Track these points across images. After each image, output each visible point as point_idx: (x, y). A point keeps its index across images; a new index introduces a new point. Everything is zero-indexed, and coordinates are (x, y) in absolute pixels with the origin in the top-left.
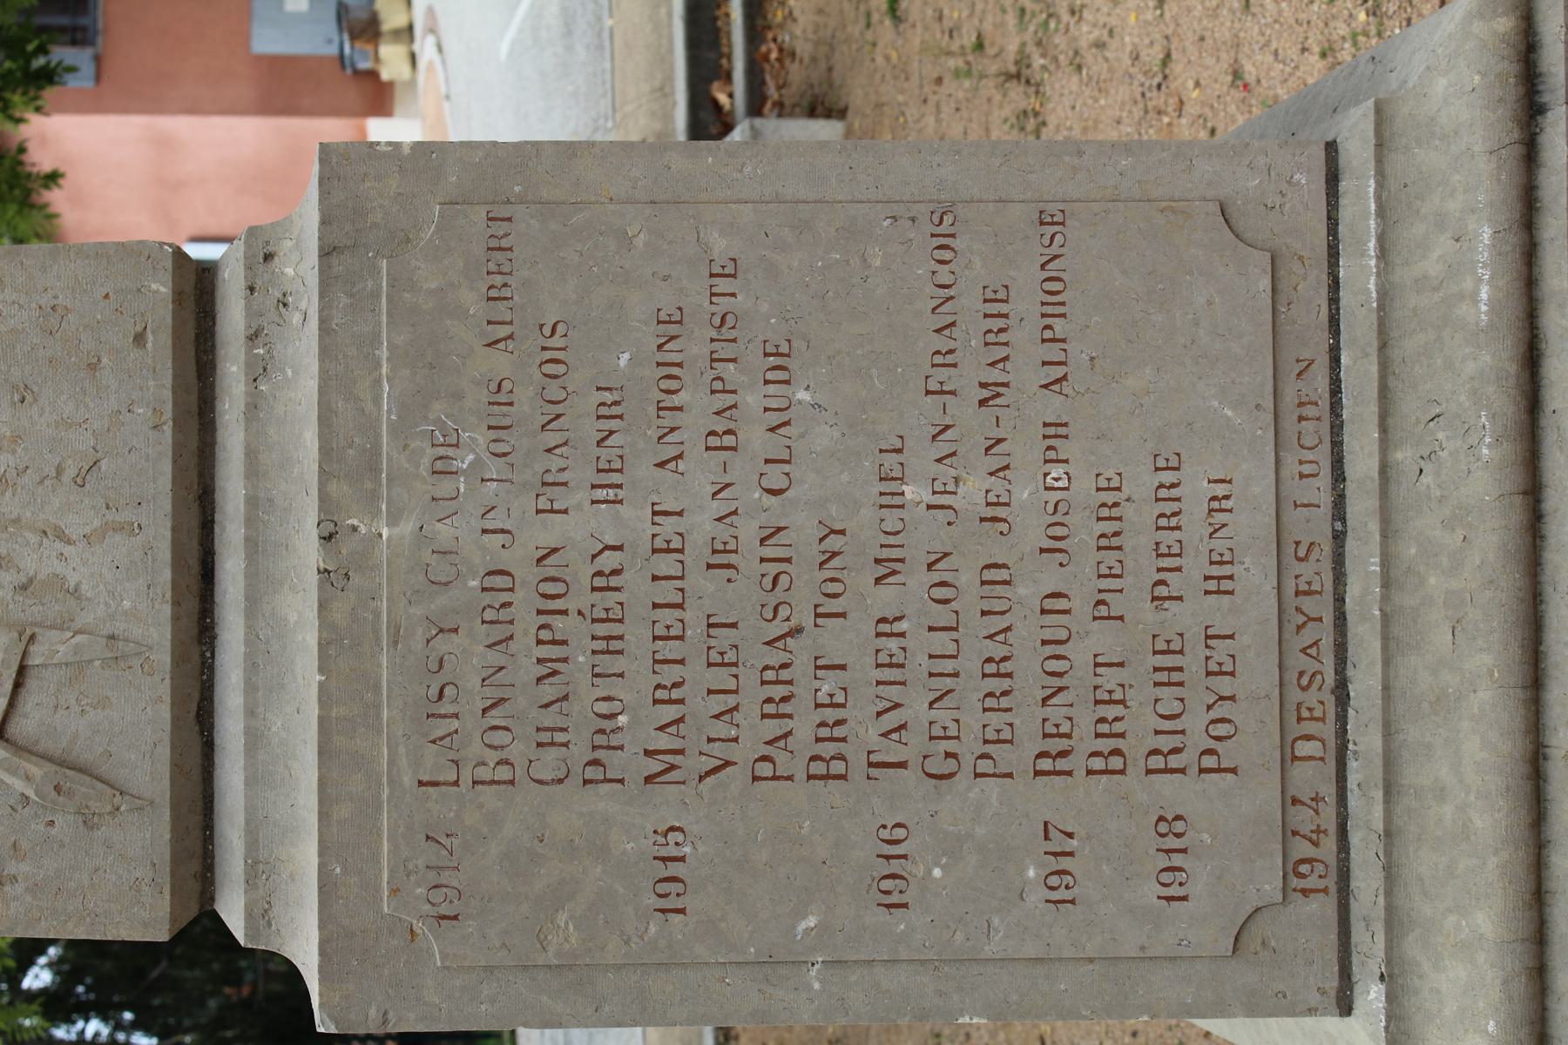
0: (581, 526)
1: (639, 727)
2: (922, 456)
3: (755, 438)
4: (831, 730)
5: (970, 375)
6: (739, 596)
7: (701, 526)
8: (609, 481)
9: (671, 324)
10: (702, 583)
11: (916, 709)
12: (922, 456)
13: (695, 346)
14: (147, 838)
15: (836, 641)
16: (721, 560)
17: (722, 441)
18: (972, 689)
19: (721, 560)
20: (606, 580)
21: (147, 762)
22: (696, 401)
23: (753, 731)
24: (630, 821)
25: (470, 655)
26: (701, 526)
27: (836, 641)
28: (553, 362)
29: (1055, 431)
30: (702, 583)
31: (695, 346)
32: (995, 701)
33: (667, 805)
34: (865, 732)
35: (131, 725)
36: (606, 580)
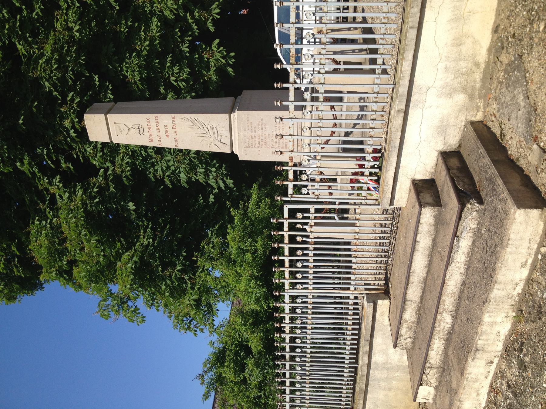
0: (253, 134)
1: (257, 145)
2: (274, 130)
3: (264, 129)
4: (269, 145)
5: (277, 126)
6: (263, 138)
7: (261, 134)
8: (255, 131)
9: (259, 122)
10: (261, 138)
11: (274, 144)
12: (274, 130)
13: (260, 124)
14: (229, 147)
15: (269, 140)
16: (262, 136)
17: (262, 129)
18: (278, 143)
19: (262, 136)
20: (255, 137)
21: (229, 144)
22: (260, 127)
23: (264, 145)
24: (257, 150)
25: (247, 140)
26: (261, 134)
27: (269, 140)
28: (251, 125)
29: (283, 129)
30: (261, 138)
31: (260, 124)
32: (279, 144)
33: (259, 149)
34: (271, 145)
35: (228, 141)
36: (255, 137)
